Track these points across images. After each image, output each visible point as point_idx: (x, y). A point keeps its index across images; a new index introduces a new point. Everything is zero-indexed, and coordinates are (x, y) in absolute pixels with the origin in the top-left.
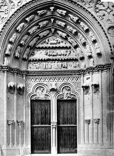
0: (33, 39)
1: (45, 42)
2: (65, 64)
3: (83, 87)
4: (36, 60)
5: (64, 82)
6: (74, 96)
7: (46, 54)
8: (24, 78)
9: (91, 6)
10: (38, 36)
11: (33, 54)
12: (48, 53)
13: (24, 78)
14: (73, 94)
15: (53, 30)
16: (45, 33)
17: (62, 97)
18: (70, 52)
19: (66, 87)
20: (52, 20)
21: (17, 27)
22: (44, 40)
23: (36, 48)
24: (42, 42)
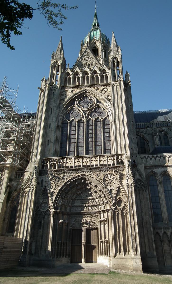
0: (74, 195)
1: (80, 196)
2: (90, 208)
3: (99, 221)
4: (75, 206)
5: (90, 218)
6: (95, 226)
7: (81, 203)
8: (69, 217)
9: (101, 179)
10: (76, 193)
11: (73, 203)
12: (82, 203)
13: (69, 217)
14: (95, 225)
15: (84, 190)
16: (80, 192)
17: (89, 227)
18: (93, 201)
19: (91, 221)
20: (83, 185)
21: (65, 191)
22: (80, 196)
23: (76, 200)
24: (79, 196)
